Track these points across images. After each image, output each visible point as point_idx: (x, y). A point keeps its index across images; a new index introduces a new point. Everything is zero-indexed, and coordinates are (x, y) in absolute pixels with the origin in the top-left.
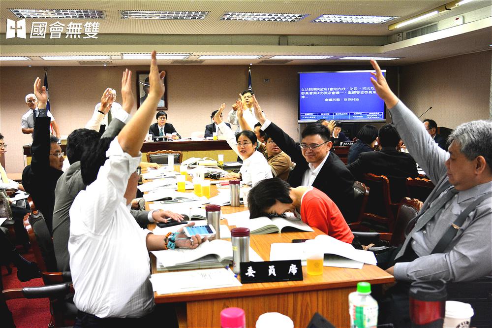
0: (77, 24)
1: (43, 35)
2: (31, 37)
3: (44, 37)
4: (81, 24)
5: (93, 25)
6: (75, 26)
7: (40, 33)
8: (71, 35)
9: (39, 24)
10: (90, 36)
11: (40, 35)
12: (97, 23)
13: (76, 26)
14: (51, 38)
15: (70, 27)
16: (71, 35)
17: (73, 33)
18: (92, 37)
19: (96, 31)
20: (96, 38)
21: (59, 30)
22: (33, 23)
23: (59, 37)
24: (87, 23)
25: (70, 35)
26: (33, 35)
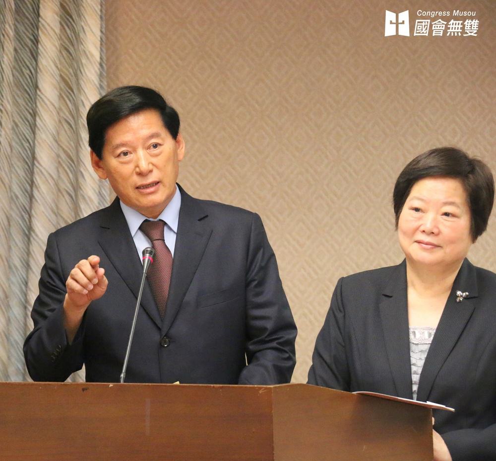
0: (457, 22)
1: (426, 33)
2: (415, 34)
3: (427, 35)
4: (462, 22)
5: (473, 23)
6: (456, 23)
7: (423, 31)
9: (422, 22)
10: (470, 34)
11: (423, 33)
12: (477, 21)
13: (457, 24)
17: (453, 30)
18: (472, 34)
19: (475, 29)
20: (476, 35)
21: (441, 28)
22: (417, 21)
23: (441, 35)
24: (467, 21)
25: (451, 32)
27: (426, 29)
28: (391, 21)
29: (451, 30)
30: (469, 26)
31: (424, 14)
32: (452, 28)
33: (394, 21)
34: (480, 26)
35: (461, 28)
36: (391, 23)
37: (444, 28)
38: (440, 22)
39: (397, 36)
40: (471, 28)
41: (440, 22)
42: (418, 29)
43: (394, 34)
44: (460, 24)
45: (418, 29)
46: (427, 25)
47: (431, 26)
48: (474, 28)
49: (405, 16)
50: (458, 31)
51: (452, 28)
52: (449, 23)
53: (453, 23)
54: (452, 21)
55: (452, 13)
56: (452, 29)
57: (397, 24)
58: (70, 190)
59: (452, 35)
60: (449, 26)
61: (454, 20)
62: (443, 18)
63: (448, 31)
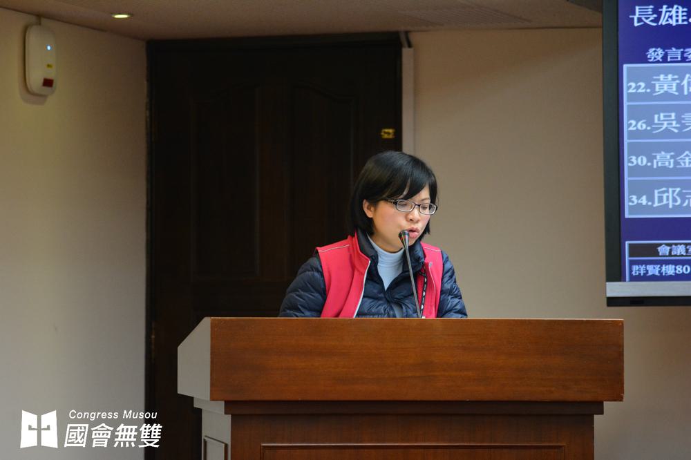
0: (129, 427)
1: (82, 443)
2: (66, 445)
3: (84, 445)
4: (136, 427)
5: (153, 429)
6: (127, 429)
7: (79, 440)
8: (122, 444)
9: (76, 428)
10: (148, 445)
11: (78, 443)
12: (159, 426)
14: (94, 446)
15: (121, 431)
16: (122, 444)
17: (124, 439)
18: (152, 445)
20: (157, 446)
21: (105, 436)
22: (69, 426)
23: (105, 446)
25: (120, 442)
26: (68, 443)
27: (83, 437)
29: (119, 439)
30: (147, 434)
31: (80, 415)
32: (122, 436)
33: (35, 426)
34: (163, 432)
35: (135, 437)
37: (109, 437)
38: (103, 427)
40: (150, 435)
41: (103, 427)
42: (71, 437)
43: (36, 444)
44: (134, 430)
45: (71, 437)
46: (84, 432)
47: (90, 432)
48: (154, 435)
49: (50, 419)
50: (130, 440)
51: (122, 436)
52: (118, 430)
53: (123, 430)
54: (122, 426)
55: (121, 415)
56: (122, 437)
57: (39, 429)
58: (437, 291)
59: (122, 445)
60: (116, 433)
61: (125, 425)
62: (108, 422)
63: (116, 440)
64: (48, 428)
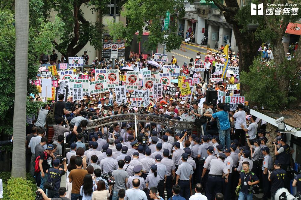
0: (288, 9)
2: (266, 14)
3: (272, 15)
4: (290, 9)
9: (270, 9)
10: (294, 14)
11: (270, 14)
12: (298, 8)
14: (276, 15)
17: (286, 13)
18: (295, 14)
19: (297, 12)
20: (297, 15)
22: (267, 8)
23: (279, 15)
25: (284, 14)
27: (272, 12)
28: (254, 8)
30: (293, 11)
33: (256, 8)
35: (289, 12)
36: (254, 8)
37: (281, 12)
39: (257, 16)
43: (256, 14)
47: (274, 11)
49: (261, 6)
55: (285, 4)
57: (257, 9)
59: (285, 15)
60: (283, 11)
64: (260, 9)
